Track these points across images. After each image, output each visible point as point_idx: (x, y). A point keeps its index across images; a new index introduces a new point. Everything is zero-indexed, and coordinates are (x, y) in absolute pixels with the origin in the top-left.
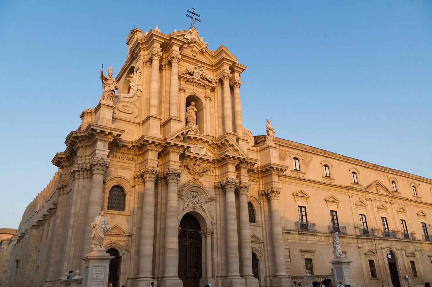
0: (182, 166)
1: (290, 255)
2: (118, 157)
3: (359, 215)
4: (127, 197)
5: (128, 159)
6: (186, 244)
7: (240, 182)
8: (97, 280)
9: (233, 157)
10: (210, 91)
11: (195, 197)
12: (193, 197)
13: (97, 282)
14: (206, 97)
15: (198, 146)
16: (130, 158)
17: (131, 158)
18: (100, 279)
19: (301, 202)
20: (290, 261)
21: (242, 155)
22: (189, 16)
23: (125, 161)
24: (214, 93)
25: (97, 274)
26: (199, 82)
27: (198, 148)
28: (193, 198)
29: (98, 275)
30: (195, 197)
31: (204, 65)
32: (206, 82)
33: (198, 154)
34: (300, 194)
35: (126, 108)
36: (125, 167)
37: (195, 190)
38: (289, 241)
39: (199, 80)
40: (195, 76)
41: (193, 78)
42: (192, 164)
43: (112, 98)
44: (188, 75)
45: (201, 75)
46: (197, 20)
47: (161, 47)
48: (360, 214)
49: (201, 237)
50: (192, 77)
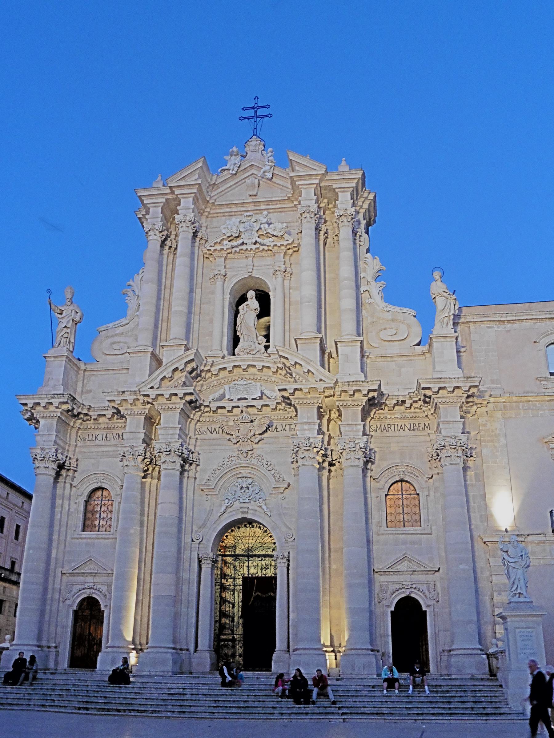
0: (217, 429)
2: (100, 437)
11: (248, 488)
12: (242, 488)
21: (321, 380)
22: (245, 118)
23: (113, 442)
26: (254, 247)
27: (241, 388)
28: (242, 491)
31: (273, 205)
33: (246, 399)
35: (115, 346)
36: (111, 453)
37: (245, 475)
39: (255, 243)
40: (245, 238)
41: (243, 243)
42: (231, 423)
46: (262, 117)
50: (240, 241)
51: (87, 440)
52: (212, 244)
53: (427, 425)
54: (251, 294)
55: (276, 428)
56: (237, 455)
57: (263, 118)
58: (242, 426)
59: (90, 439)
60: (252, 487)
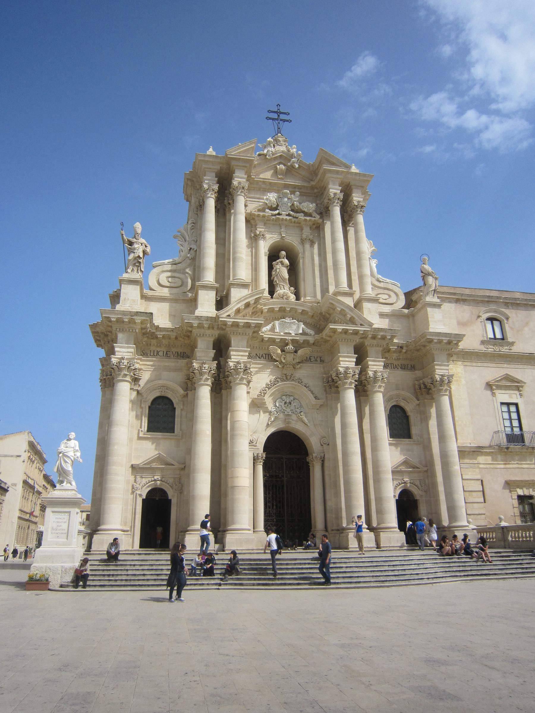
0: (264, 355)
1: (483, 491)
2: (161, 353)
3: (499, 404)
4: (177, 412)
5: (176, 355)
6: (283, 478)
7: (363, 371)
8: (58, 531)
9: (345, 332)
10: (311, 228)
11: (290, 403)
12: (285, 403)
13: (57, 533)
14: (303, 242)
15: (287, 321)
16: (179, 353)
17: (181, 353)
18: (62, 530)
19: (507, 395)
20: (483, 501)
22: (270, 119)
24: (320, 232)
25: (58, 522)
26: (288, 218)
28: (286, 405)
29: (60, 524)
30: (290, 403)
32: (301, 216)
34: (504, 383)
38: (482, 466)
41: (279, 214)
43: (139, 268)
44: (267, 210)
45: (290, 207)
46: (284, 121)
47: (216, 177)
48: (502, 404)
49: (309, 466)
51: (149, 355)
52: (256, 210)
53: (413, 366)
54: (283, 253)
55: (310, 359)
56: (281, 378)
57: (284, 121)
58: (288, 355)
59: (152, 354)
60: (294, 403)
